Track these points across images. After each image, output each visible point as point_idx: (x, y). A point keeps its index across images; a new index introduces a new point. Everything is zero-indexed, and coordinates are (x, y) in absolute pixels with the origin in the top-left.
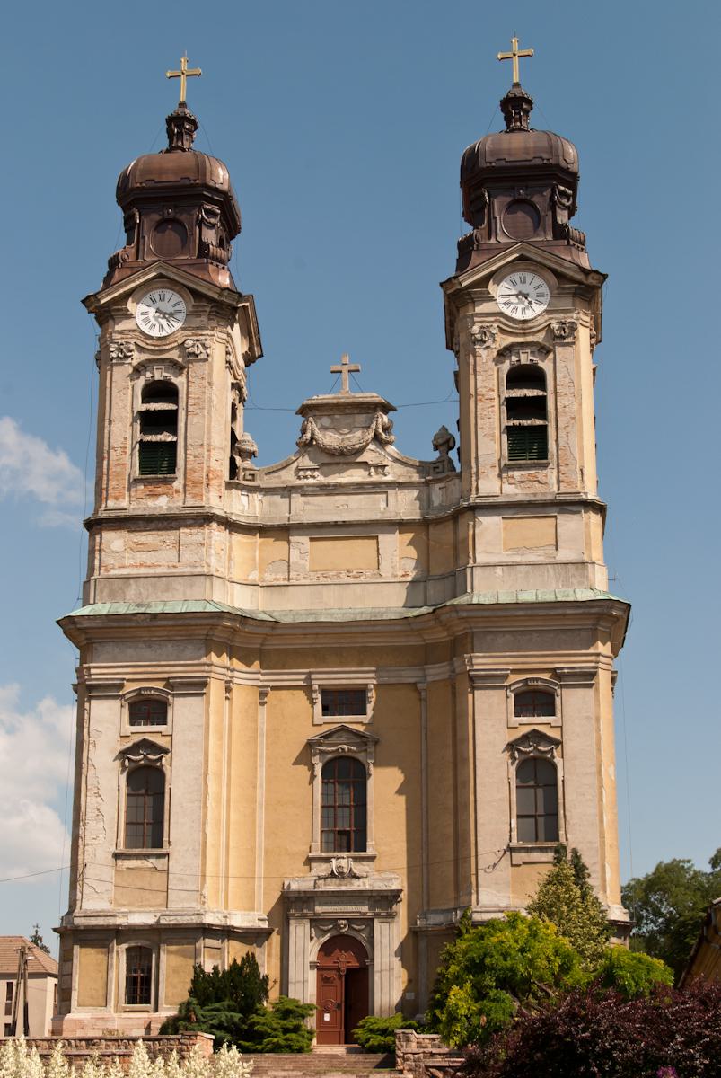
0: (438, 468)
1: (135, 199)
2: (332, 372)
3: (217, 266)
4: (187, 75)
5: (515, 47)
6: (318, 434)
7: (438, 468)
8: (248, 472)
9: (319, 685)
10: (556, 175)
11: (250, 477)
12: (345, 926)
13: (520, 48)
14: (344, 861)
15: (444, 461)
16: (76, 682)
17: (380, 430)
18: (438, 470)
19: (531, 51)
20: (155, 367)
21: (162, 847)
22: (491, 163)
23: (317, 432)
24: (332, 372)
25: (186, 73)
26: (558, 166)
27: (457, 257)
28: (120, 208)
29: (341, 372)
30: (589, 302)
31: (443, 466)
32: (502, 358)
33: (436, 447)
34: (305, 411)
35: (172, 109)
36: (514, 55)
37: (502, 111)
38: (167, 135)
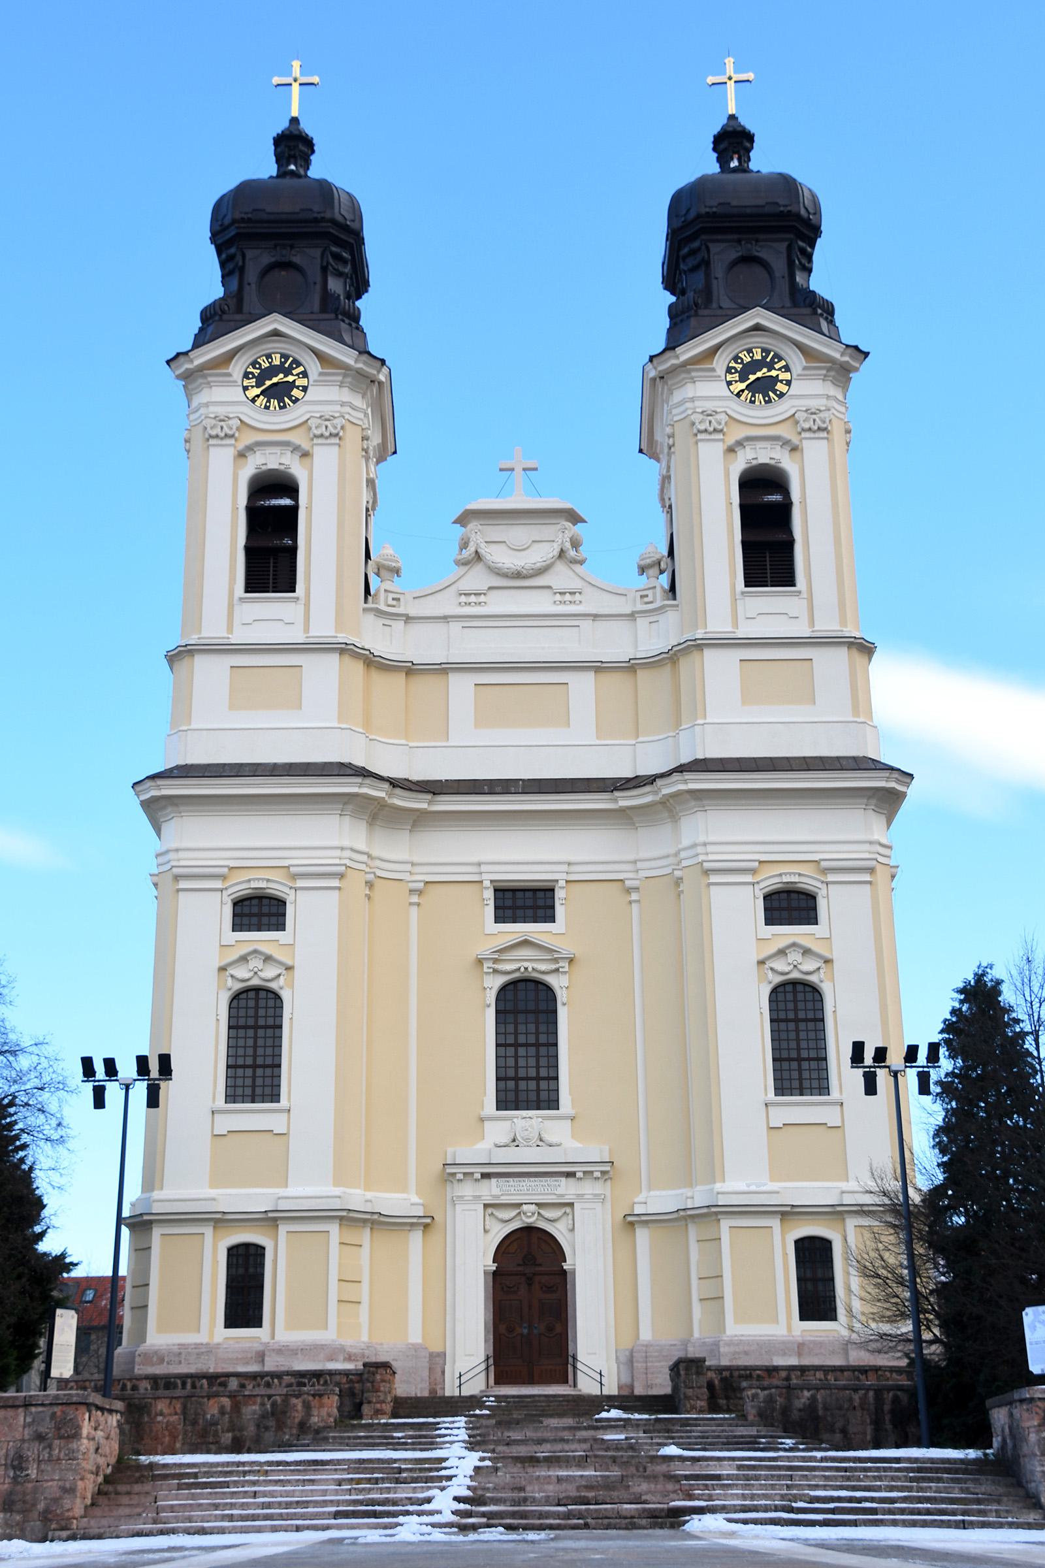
0: (647, 596)
1: (238, 235)
2: (501, 470)
3: (350, 325)
4: (300, 84)
5: (730, 70)
6: (485, 550)
7: (647, 596)
8: (391, 596)
9: (492, 881)
10: (795, 226)
11: (394, 603)
12: (533, 1214)
13: (735, 72)
14: (527, 1121)
15: (655, 587)
16: (156, 871)
17: (568, 545)
18: (646, 600)
19: (750, 76)
20: (267, 452)
21: (278, 1101)
22: (711, 207)
23: (483, 545)
24: (501, 470)
25: (299, 81)
26: (798, 215)
27: (668, 326)
28: (213, 247)
29: (513, 470)
30: (843, 388)
31: (654, 595)
32: (732, 455)
33: (642, 570)
34: (464, 519)
35: (282, 125)
36: (730, 78)
37: (714, 149)
38: (274, 158)
